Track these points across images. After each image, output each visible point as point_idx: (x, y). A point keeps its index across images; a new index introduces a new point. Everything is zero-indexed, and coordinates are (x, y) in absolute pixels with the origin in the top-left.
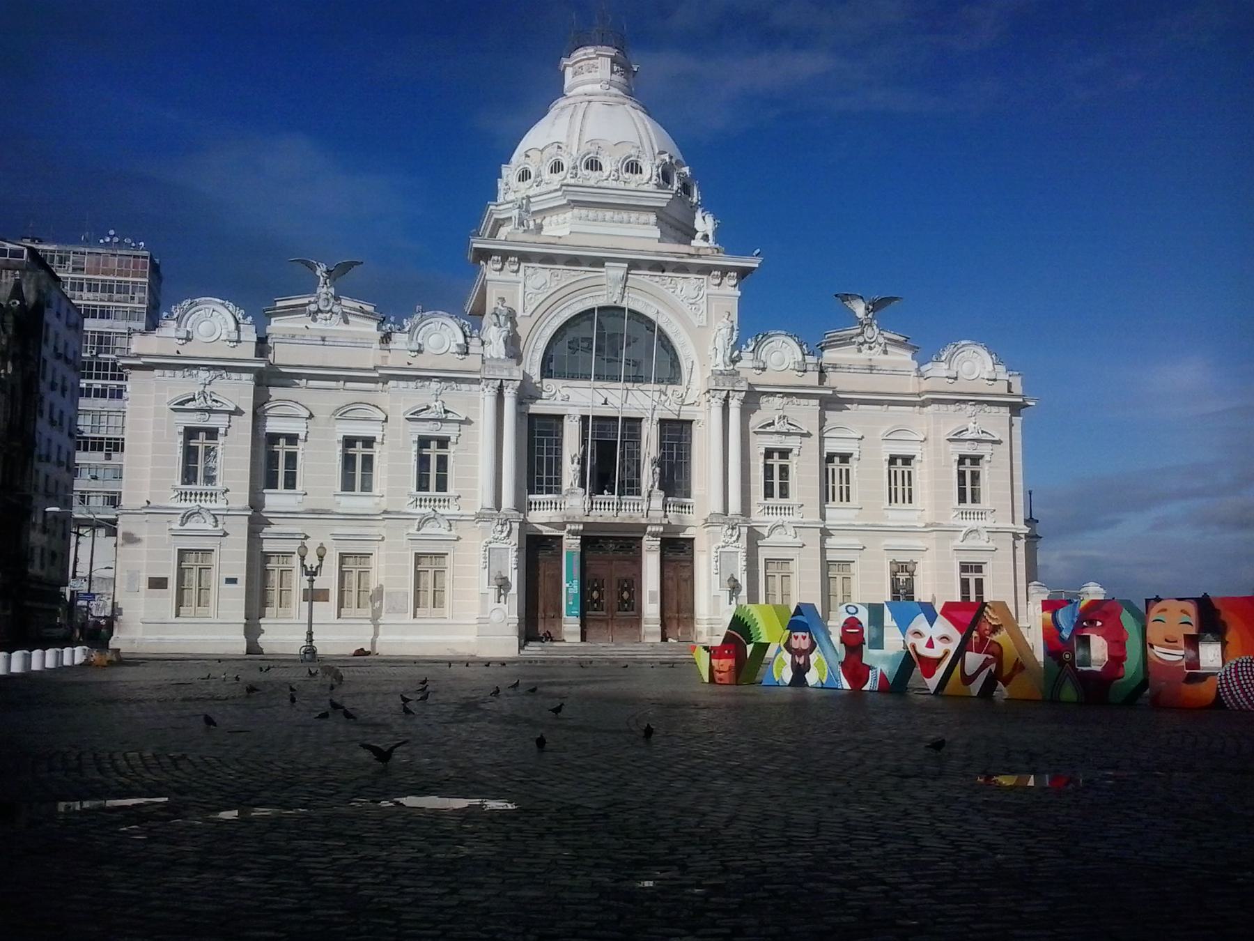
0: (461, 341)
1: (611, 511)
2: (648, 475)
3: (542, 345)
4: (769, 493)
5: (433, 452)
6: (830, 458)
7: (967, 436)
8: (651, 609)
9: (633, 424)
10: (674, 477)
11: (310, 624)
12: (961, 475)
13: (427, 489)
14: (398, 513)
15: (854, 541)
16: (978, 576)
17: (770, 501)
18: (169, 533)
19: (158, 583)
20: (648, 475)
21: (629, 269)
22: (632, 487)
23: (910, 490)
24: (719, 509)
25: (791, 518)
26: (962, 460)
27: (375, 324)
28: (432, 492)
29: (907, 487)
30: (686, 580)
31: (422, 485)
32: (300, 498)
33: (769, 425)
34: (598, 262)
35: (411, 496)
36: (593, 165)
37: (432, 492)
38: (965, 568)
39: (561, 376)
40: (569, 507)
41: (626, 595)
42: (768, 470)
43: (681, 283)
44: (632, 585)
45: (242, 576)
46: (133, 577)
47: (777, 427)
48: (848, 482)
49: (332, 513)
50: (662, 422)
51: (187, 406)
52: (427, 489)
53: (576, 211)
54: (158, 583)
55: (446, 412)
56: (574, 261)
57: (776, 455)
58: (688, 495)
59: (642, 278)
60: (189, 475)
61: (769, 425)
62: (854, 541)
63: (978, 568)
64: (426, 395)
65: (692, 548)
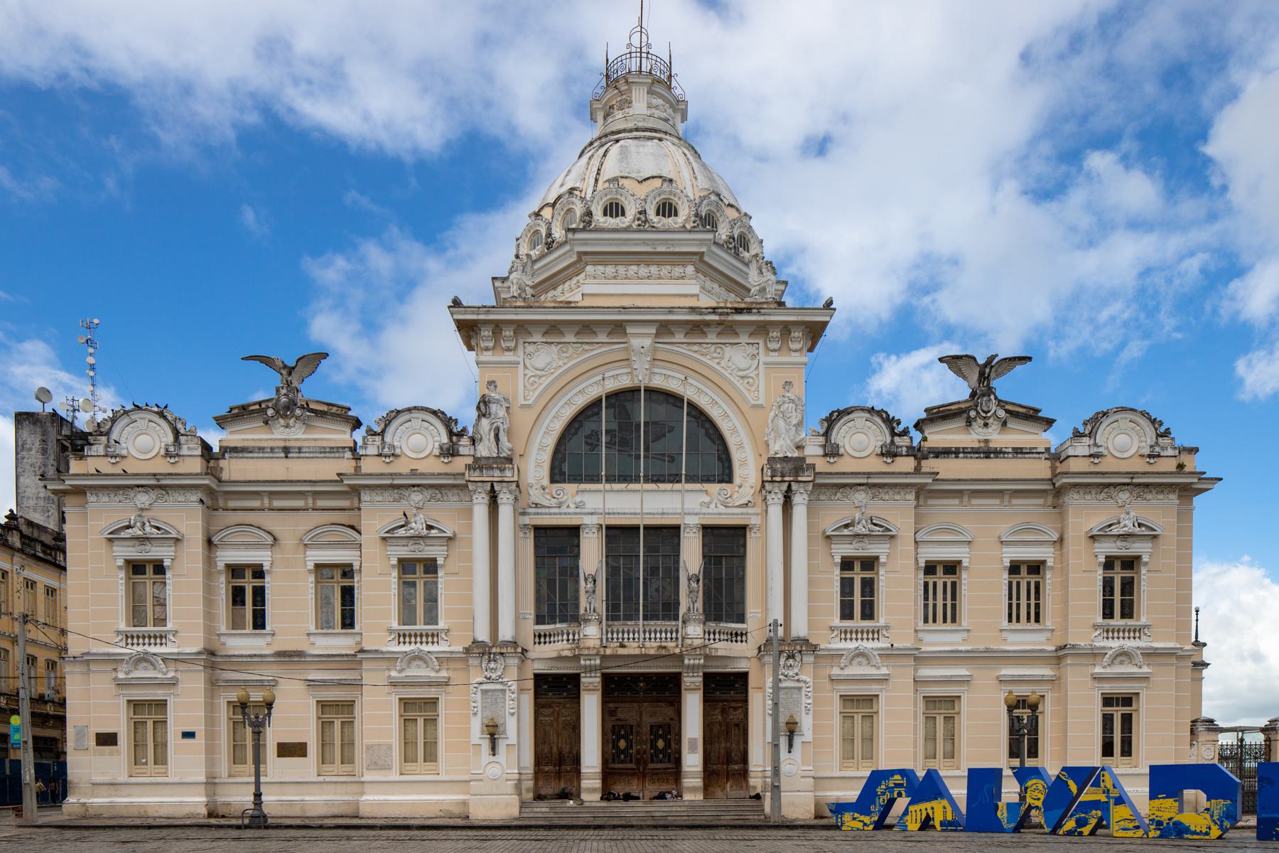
0: (445, 439)
1: (641, 643)
2: (689, 599)
7: (1116, 530)
8: (692, 761)
9: (673, 532)
12: (1108, 585)
14: (376, 651)
15: (961, 671)
16: (1126, 710)
19: (107, 740)
20: (689, 599)
21: (657, 335)
22: (667, 609)
23: (1037, 606)
26: (1109, 564)
29: (1033, 602)
30: (737, 725)
35: (390, 631)
36: (614, 209)
43: (728, 350)
44: (671, 730)
45: (200, 729)
46: (80, 734)
47: (859, 529)
48: (954, 597)
50: (706, 528)
51: (123, 535)
53: (589, 269)
54: (107, 740)
55: (430, 527)
56: (586, 328)
57: (857, 566)
58: (741, 618)
60: (137, 615)
61: (846, 526)
62: (961, 671)
63: (1127, 701)
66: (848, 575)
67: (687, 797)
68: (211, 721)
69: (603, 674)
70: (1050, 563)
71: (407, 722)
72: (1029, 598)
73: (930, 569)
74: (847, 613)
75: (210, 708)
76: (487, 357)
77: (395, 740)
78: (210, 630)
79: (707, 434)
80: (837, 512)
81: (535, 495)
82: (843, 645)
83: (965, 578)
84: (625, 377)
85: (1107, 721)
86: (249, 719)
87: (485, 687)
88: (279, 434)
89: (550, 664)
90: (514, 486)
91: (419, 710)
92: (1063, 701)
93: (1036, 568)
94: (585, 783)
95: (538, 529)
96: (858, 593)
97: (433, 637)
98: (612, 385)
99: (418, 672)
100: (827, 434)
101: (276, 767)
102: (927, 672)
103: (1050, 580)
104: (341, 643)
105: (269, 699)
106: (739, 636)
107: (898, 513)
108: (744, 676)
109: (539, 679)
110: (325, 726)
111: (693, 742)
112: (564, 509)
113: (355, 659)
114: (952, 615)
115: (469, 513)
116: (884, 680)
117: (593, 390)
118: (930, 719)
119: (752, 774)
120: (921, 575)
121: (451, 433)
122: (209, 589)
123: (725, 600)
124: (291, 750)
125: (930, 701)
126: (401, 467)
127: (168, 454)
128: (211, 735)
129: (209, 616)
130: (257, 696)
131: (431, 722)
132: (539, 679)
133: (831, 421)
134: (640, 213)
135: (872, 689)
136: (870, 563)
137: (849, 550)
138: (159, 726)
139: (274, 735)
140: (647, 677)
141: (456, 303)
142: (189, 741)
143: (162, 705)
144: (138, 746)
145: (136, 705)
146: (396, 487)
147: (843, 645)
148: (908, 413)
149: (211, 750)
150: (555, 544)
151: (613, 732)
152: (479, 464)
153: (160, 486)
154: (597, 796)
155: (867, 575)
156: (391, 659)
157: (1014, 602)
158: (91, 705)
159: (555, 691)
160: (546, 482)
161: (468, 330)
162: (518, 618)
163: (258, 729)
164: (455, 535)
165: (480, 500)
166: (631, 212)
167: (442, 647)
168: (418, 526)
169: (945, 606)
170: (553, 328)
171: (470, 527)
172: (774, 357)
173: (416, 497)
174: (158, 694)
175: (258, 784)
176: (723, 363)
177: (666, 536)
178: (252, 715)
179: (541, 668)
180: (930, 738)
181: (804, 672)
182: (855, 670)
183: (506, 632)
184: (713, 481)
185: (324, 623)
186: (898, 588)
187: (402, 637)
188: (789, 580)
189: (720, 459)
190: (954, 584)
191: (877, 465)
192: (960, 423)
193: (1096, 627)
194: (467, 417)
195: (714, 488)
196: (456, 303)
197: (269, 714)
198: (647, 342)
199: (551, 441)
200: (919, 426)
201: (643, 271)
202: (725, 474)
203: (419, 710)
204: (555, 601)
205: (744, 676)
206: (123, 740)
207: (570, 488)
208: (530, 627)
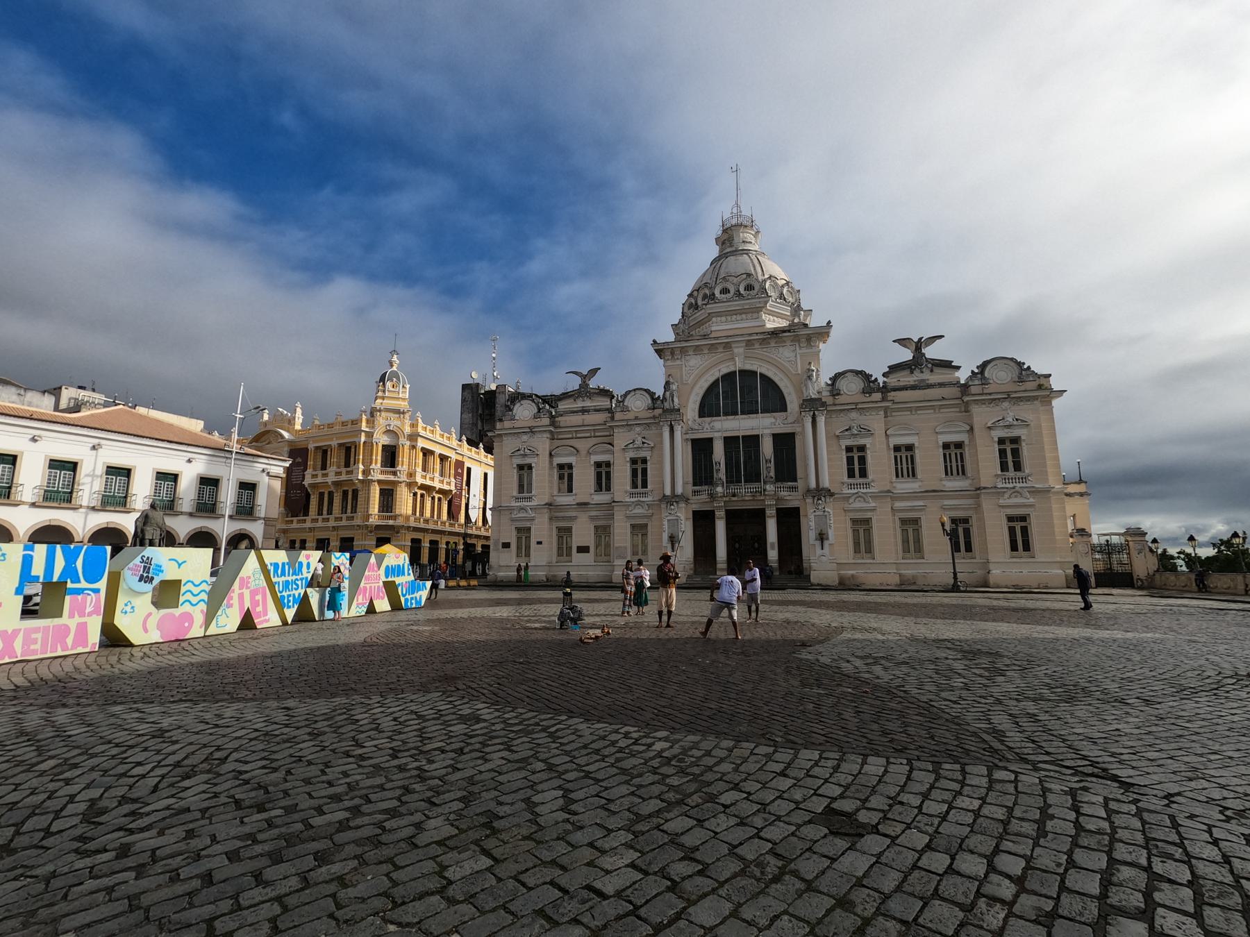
1: (745, 495)
5: (639, 467)
10: (787, 468)
16: (1023, 524)
17: (851, 481)
19: (506, 545)
22: (754, 476)
31: (634, 485)
38: (1010, 519)
39: (710, 415)
58: (795, 480)
59: (758, 350)
60: (521, 488)
63: (1023, 518)
64: (636, 434)
70: (967, 442)
73: (897, 449)
74: (851, 474)
76: (669, 363)
77: (628, 545)
80: (841, 422)
83: (918, 455)
85: (1012, 531)
88: (580, 404)
92: (981, 520)
93: (959, 445)
94: (719, 566)
95: (694, 441)
96: (857, 463)
98: (725, 371)
99: (638, 511)
100: (833, 385)
101: (578, 558)
102: (898, 504)
103: (967, 452)
104: (603, 498)
106: (794, 489)
107: (876, 422)
109: (695, 513)
111: (772, 544)
114: (913, 474)
115: (661, 435)
116: (873, 510)
117: (715, 374)
118: (904, 531)
121: (653, 399)
122: (551, 475)
124: (583, 549)
125: (904, 522)
126: (630, 416)
127: (535, 418)
131: (645, 535)
132: (694, 512)
133: (835, 378)
135: (868, 515)
136: (862, 448)
137: (849, 442)
141: (655, 341)
143: (529, 529)
144: (519, 548)
145: (519, 530)
146: (629, 426)
148: (877, 372)
150: (701, 448)
152: (665, 411)
153: (532, 431)
156: (627, 505)
159: (703, 521)
161: (660, 352)
162: (685, 483)
166: (732, 292)
167: (650, 498)
171: (662, 442)
172: (804, 350)
173: (638, 429)
174: (528, 524)
177: (753, 441)
178: (564, 533)
179: (696, 507)
180: (905, 541)
181: (830, 507)
182: (858, 505)
183: (679, 490)
185: (599, 488)
186: (880, 462)
188: (822, 460)
192: (907, 372)
193: (997, 476)
194: (659, 392)
196: (655, 341)
198: (741, 350)
199: (699, 399)
200: (884, 375)
201: (739, 317)
202: (783, 408)
204: (702, 472)
207: (708, 419)
208: (690, 488)
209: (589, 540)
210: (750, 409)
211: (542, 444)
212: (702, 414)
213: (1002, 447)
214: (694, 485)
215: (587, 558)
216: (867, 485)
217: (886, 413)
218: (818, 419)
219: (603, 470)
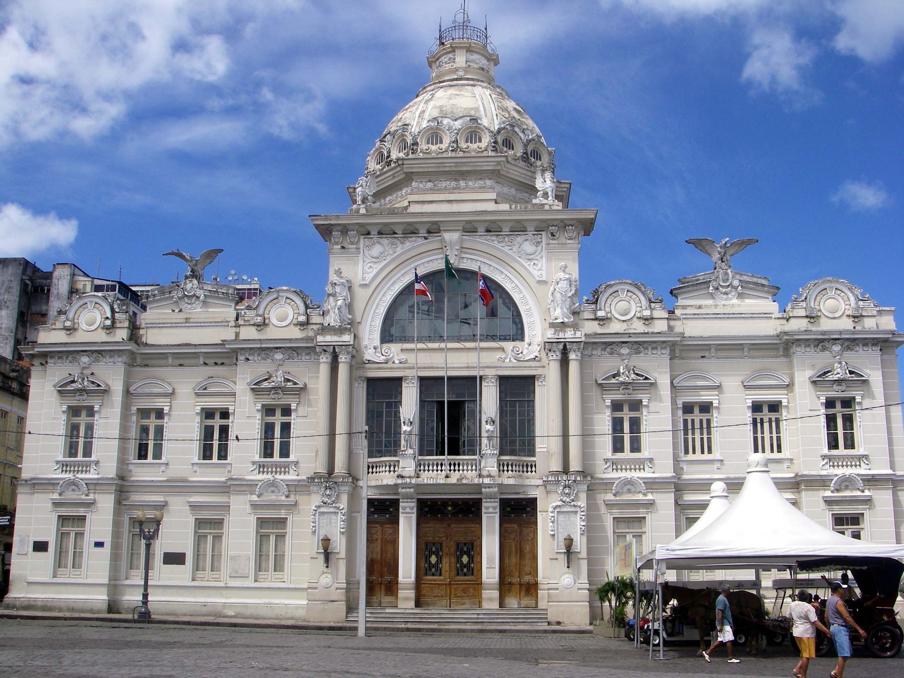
3: (382, 310)
4: (618, 447)
6: (688, 408)
8: (490, 572)
11: (146, 586)
13: (271, 456)
18: (51, 501)
19: (40, 547)
23: (779, 439)
24: (556, 466)
25: (643, 474)
27: (233, 305)
28: (276, 458)
29: (774, 435)
32: (163, 468)
33: (614, 376)
34: (434, 229)
37: (276, 458)
40: (411, 471)
41: (433, 559)
42: (617, 425)
45: (108, 540)
49: (187, 481)
52: (271, 456)
54: (40, 547)
58: (532, 453)
59: (481, 241)
61: (614, 376)
65: (535, 509)
66: (618, 415)
67: (485, 605)
68: (116, 534)
69: (418, 500)
71: (262, 539)
72: (771, 432)
75: (117, 524)
78: (122, 462)
79: (504, 303)
81: (369, 355)
82: (615, 475)
84: (440, 261)
86: (144, 532)
87: (322, 510)
89: (377, 491)
90: (350, 349)
91: (271, 527)
97: (285, 468)
101: (162, 574)
105: (159, 517)
108: (534, 501)
110: (199, 539)
112: (390, 365)
113: (225, 488)
119: (540, 586)
120: (680, 412)
123: (517, 438)
128: (116, 546)
129: (122, 450)
130: (150, 514)
134: (453, 142)
138: (79, 537)
139: (161, 546)
140: (454, 502)
142: (99, 549)
147: (615, 475)
149: (115, 557)
151: (425, 549)
154: (412, 604)
155: (634, 414)
157: (759, 435)
158: (34, 518)
160: (377, 342)
163: (150, 538)
164: (305, 385)
165: (324, 360)
167: (291, 476)
168: (278, 378)
169: (702, 439)
170: (386, 232)
175: (146, 586)
176: (515, 249)
177: (468, 385)
178: (146, 529)
184: (509, 340)
187: (261, 468)
189: (514, 322)
190: (709, 421)
191: (639, 327)
195: (508, 345)
197: (158, 529)
202: (518, 334)
203: (271, 527)
204: (382, 438)
205: (534, 501)
206: (52, 547)
209: (186, 545)
210: (464, 331)
211: (112, 375)
212: (387, 337)
213: (831, 411)
214: (369, 457)
215: (180, 574)
216: (640, 465)
217: (672, 351)
218: (572, 356)
219: (217, 422)
